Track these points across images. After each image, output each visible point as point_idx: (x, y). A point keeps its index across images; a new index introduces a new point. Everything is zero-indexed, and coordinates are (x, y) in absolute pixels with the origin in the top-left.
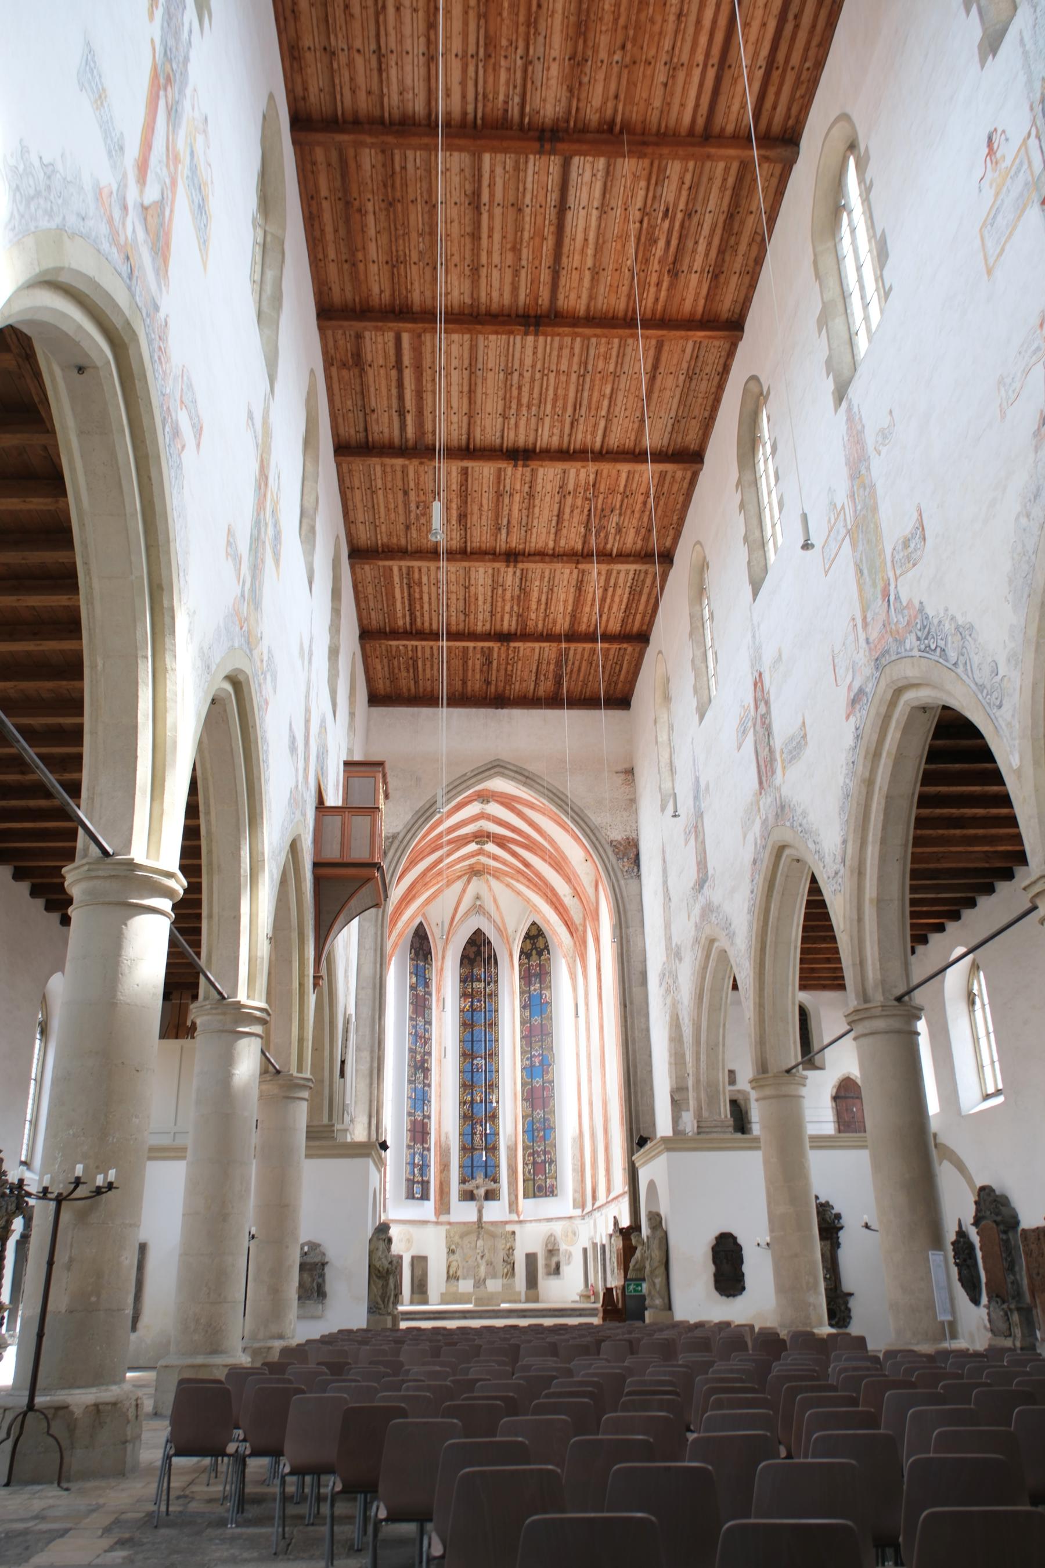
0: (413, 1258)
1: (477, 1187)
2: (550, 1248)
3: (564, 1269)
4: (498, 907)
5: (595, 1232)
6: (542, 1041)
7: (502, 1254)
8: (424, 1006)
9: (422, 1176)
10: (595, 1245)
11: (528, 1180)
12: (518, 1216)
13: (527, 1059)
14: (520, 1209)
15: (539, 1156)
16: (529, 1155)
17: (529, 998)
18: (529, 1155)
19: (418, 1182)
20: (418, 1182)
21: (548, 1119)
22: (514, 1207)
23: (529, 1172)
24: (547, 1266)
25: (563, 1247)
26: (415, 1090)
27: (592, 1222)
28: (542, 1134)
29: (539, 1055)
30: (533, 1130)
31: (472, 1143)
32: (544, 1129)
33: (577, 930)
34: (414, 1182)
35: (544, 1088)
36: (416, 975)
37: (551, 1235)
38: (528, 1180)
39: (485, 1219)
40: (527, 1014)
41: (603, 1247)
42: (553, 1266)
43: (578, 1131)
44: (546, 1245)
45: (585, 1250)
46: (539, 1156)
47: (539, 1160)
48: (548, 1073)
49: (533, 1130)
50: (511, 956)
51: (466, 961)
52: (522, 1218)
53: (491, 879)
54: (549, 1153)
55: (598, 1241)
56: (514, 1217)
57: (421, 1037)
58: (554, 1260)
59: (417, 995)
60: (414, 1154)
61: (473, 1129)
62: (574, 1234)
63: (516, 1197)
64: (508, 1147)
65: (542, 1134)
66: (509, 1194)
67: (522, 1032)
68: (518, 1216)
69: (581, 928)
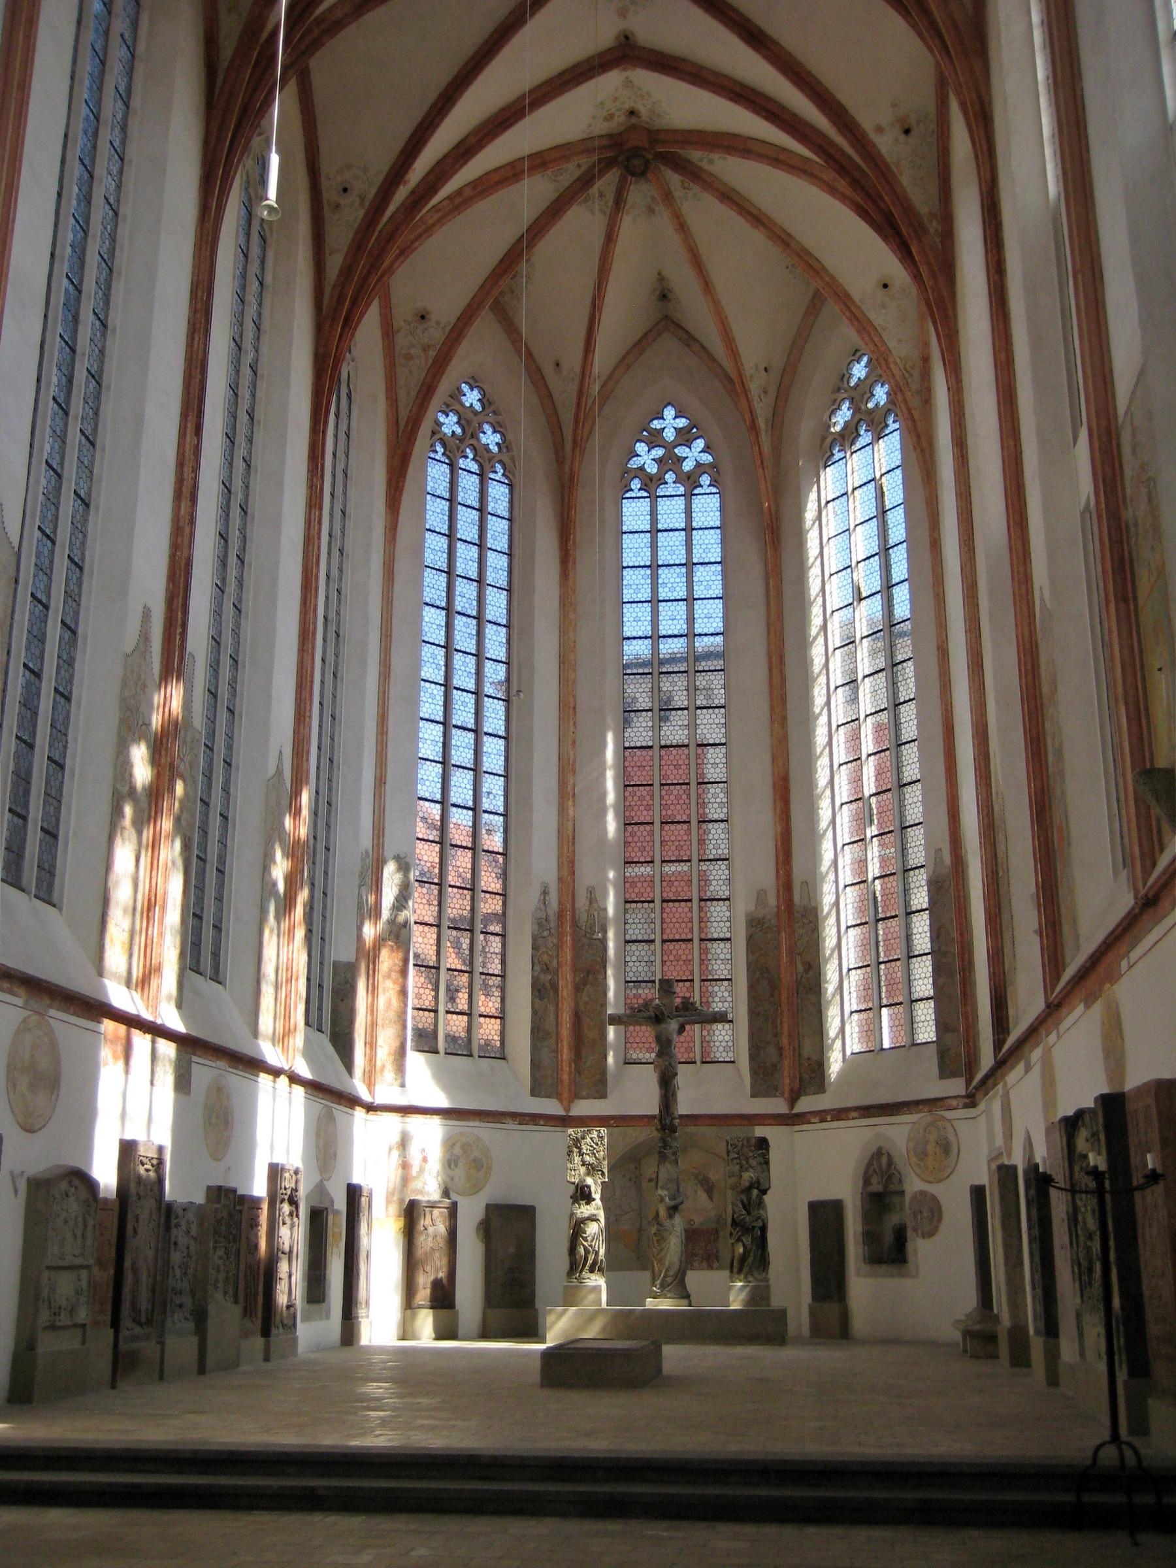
0: (490, 1208)
2: (876, 1187)
3: (921, 1248)
4: (707, 287)
5: (1009, 1135)
7: (729, 1204)
10: (1006, 1174)
24: (870, 1237)
25: (914, 1184)
27: (997, 1106)
33: (920, 229)
37: (879, 1153)
39: (684, 1106)
41: (1040, 1182)
42: (888, 1237)
43: (947, 859)
44: (867, 1181)
45: (978, 1193)
53: (674, 179)
55: (1018, 1159)
58: (894, 1219)
62: (945, 1148)
69: (933, 227)
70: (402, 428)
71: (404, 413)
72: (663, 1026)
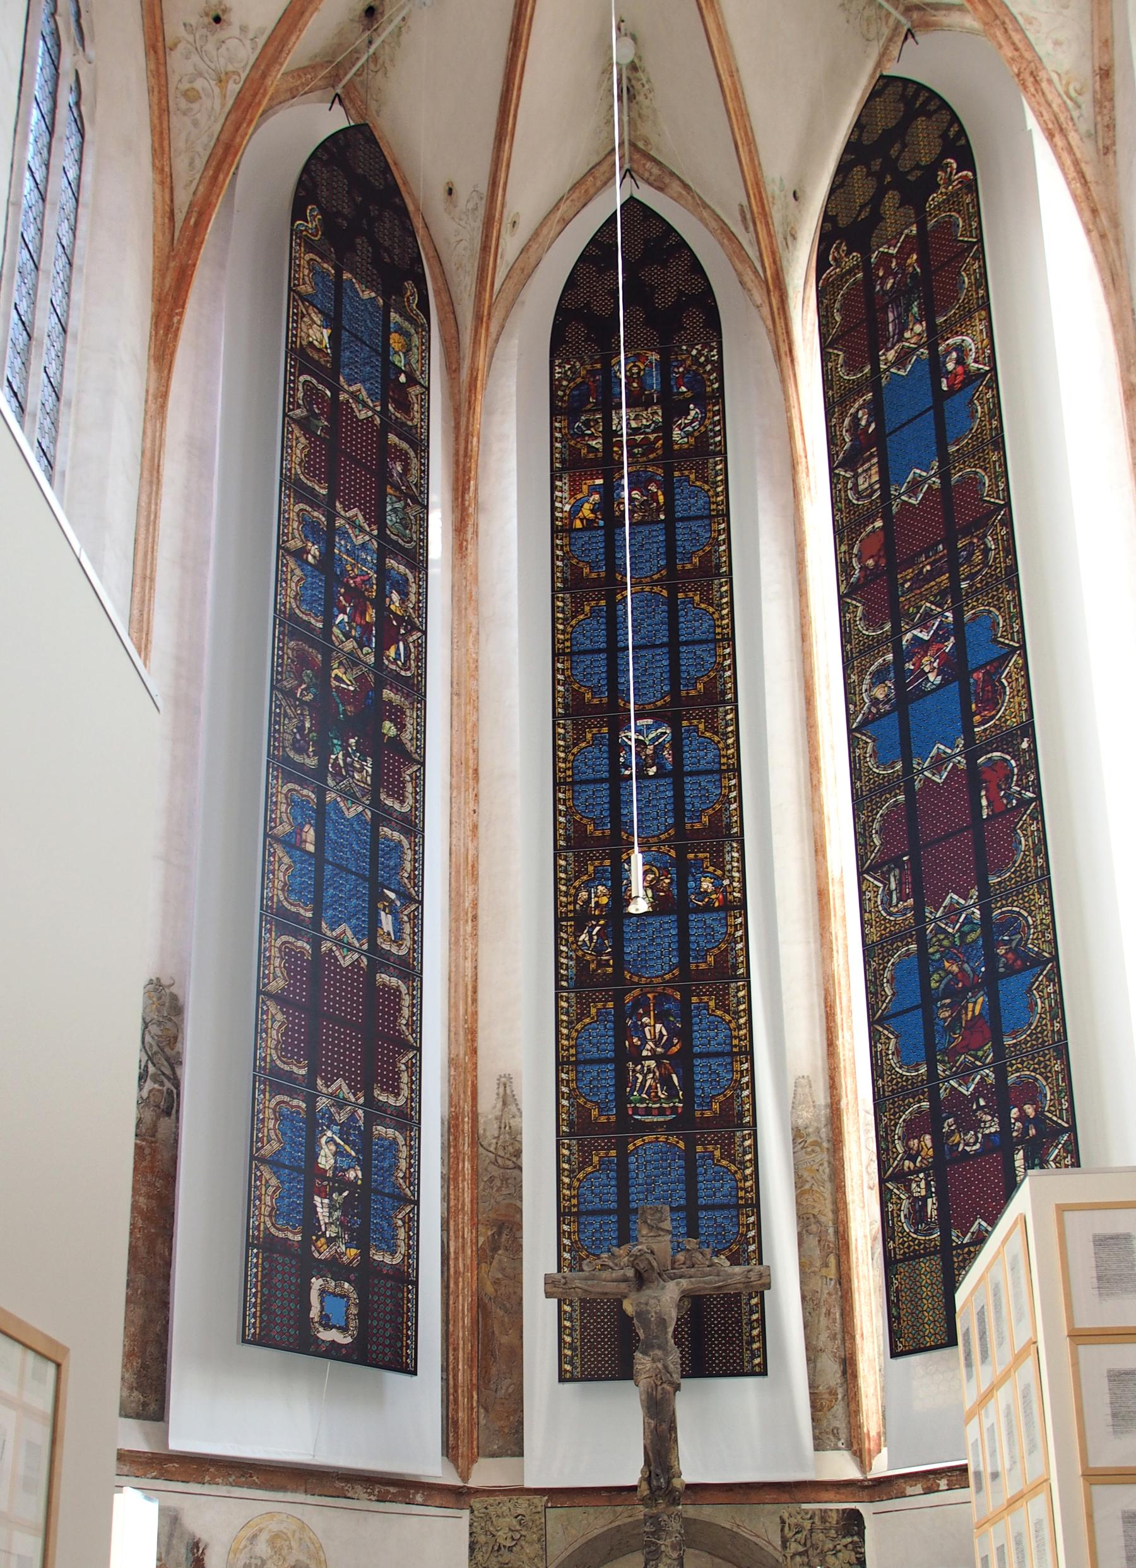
1: (641, 1280)
6: (953, 564)
8: (383, 476)
9: (361, 1240)
11: (913, 1256)
12: (861, 1457)
13: (879, 677)
14: (871, 1421)
15: (969, 1123)
16: (913, 1130)
17: (876, 410)
18: (913, 1130)
19: (335, 1268)
20: (335, 1268)
21: (1011, 923)
22: (837, 1417)
23: (918, 1214)
26: (321, 815)
28: (977, 1005)
29: (939, 637)
30: (928, 1000)
31: (622, 1099)
32: (990, 983)
34: (308, 1266)
35: (973, 778)
36: (333, 321)
38: (913, 1256)
40: (869, 477)
46: (969, 1123)
47: (970, 1143)
48: (992, 697)
49: (928, 1000)
50: (777, 287)
51: (577, 331)
52: (881, 1466)
54: (1029, 1091)
56: (842, 1467)
57: (357, 596)
59: (337, 410)
60: (313, 1125)
61: (621, 1033)
63: (848, 1366)
64: (798, 1137)
65: (977, 1005)
66: (812, 1353)
67: (843, 568)
68: (861, 1457)
70: (179, 224)
71: (183, 198)
72: (647, 1292)
